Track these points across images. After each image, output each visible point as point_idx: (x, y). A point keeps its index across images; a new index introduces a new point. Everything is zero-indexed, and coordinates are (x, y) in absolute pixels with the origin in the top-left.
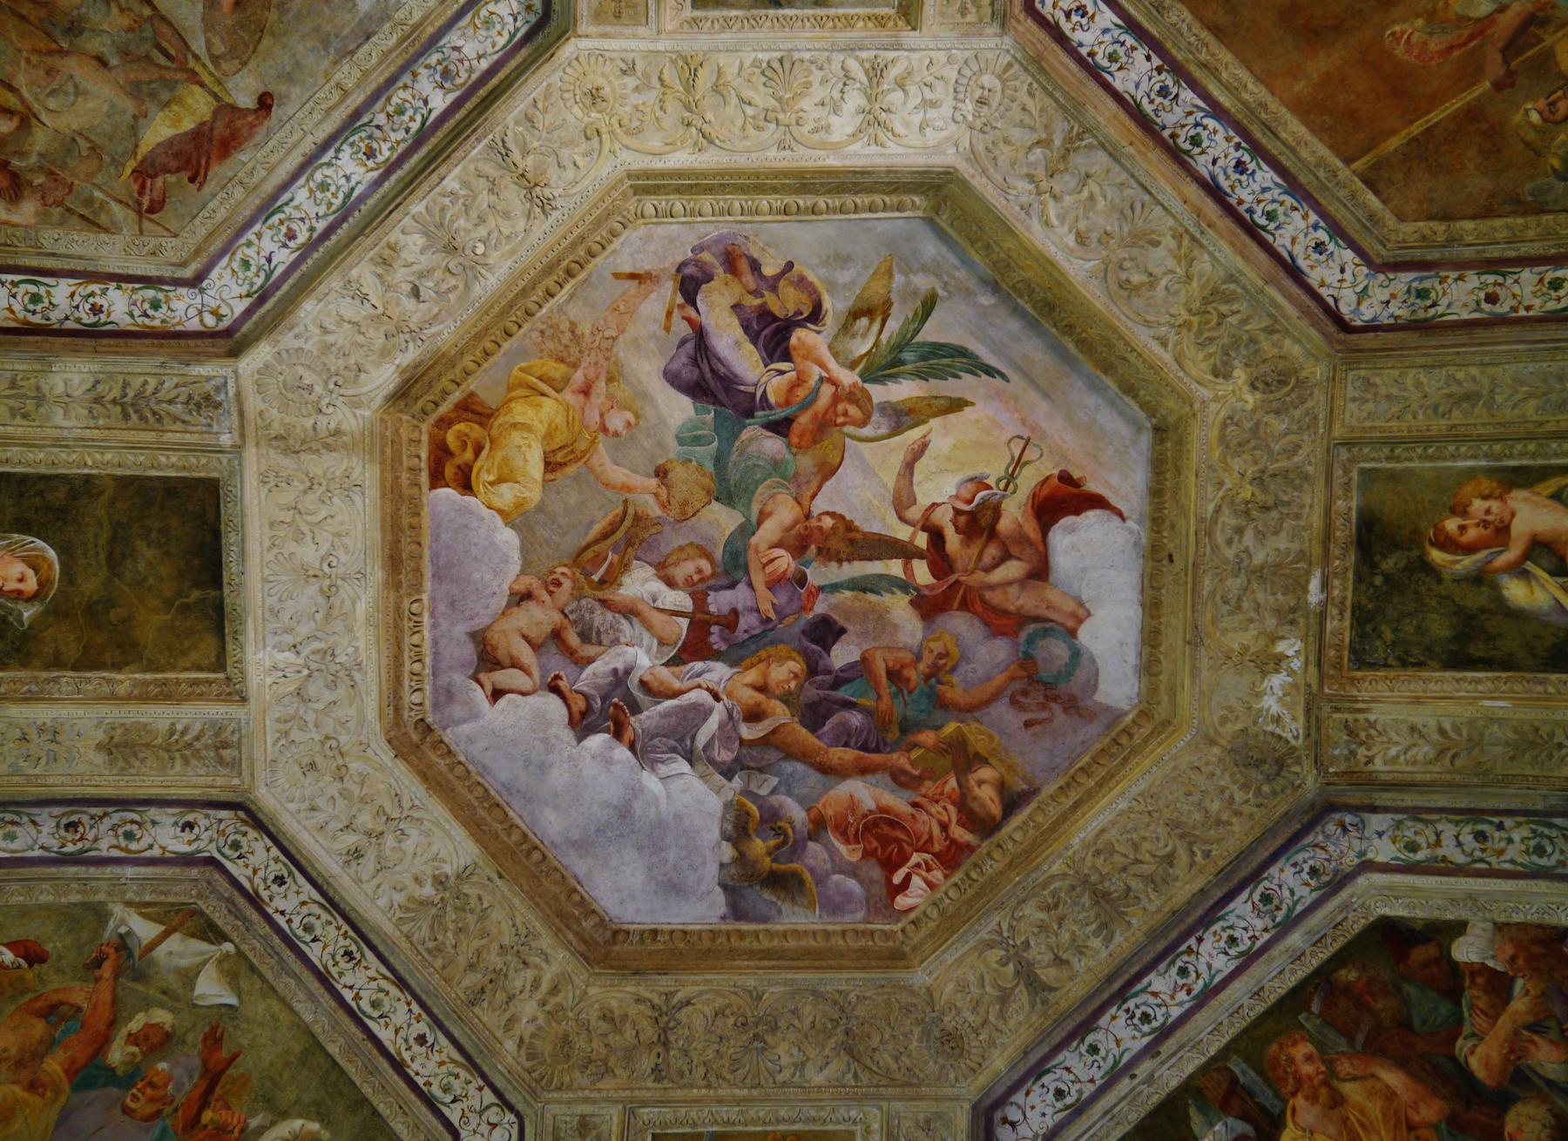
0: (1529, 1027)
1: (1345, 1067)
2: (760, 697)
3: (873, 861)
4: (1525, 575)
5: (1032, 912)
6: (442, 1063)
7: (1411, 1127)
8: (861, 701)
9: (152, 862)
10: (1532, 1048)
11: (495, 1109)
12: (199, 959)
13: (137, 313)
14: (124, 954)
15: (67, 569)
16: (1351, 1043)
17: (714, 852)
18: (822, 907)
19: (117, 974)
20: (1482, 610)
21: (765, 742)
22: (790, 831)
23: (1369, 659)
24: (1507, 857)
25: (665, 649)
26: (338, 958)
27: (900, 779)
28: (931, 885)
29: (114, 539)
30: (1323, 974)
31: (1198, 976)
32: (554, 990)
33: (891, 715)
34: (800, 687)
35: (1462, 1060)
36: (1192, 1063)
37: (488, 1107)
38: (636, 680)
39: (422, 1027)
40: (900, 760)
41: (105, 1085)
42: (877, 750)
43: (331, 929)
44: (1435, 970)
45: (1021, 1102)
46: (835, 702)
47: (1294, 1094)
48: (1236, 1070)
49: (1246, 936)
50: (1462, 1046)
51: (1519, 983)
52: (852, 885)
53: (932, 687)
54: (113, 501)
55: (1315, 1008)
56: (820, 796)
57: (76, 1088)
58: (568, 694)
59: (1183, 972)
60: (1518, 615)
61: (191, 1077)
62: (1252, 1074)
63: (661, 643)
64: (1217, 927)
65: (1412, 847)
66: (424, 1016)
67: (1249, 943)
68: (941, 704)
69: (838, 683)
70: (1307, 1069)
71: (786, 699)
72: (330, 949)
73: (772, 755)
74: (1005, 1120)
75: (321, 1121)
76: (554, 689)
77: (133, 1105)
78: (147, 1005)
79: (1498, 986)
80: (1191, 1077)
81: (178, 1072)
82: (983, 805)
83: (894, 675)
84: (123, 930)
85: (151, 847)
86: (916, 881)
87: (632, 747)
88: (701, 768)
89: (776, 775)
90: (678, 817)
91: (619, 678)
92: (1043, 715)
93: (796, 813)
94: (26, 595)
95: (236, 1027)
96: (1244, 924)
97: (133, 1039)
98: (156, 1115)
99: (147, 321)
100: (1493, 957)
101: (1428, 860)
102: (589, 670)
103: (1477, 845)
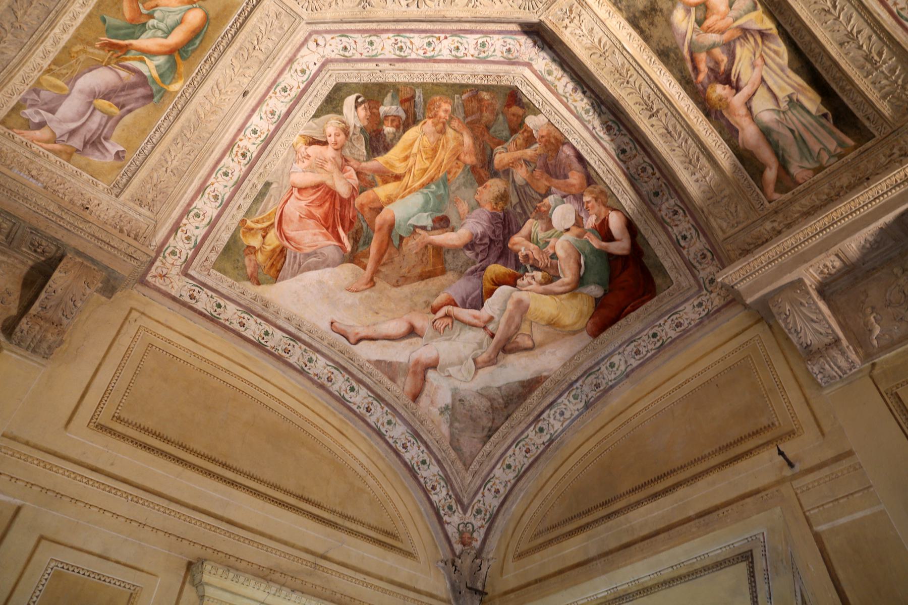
0: (525, 161)
1: (455, 124)
4: (688, 11)
7: (458, 159)
10: (520, 167)
16: (466, 117)
20: (661, 10)
24: (575, 104)
36: (402, 78)
44: (515, 119)
45: (327, 40)
47: (430, 118)
48: (417, 94)
49: (463, 51)
50: (499, 149)
51: (537, 145)
55: (464, 97)
59: (429, 44)
60: (669, 24)
62: (422, 100)
64: (456, 39)
65: (550, 73)
67: (462, 55)
70: (442, 114)
79: (530, 140)
96: (467, 47)
100: (537, 131)
101: (550, 82)
103: (571, 92)
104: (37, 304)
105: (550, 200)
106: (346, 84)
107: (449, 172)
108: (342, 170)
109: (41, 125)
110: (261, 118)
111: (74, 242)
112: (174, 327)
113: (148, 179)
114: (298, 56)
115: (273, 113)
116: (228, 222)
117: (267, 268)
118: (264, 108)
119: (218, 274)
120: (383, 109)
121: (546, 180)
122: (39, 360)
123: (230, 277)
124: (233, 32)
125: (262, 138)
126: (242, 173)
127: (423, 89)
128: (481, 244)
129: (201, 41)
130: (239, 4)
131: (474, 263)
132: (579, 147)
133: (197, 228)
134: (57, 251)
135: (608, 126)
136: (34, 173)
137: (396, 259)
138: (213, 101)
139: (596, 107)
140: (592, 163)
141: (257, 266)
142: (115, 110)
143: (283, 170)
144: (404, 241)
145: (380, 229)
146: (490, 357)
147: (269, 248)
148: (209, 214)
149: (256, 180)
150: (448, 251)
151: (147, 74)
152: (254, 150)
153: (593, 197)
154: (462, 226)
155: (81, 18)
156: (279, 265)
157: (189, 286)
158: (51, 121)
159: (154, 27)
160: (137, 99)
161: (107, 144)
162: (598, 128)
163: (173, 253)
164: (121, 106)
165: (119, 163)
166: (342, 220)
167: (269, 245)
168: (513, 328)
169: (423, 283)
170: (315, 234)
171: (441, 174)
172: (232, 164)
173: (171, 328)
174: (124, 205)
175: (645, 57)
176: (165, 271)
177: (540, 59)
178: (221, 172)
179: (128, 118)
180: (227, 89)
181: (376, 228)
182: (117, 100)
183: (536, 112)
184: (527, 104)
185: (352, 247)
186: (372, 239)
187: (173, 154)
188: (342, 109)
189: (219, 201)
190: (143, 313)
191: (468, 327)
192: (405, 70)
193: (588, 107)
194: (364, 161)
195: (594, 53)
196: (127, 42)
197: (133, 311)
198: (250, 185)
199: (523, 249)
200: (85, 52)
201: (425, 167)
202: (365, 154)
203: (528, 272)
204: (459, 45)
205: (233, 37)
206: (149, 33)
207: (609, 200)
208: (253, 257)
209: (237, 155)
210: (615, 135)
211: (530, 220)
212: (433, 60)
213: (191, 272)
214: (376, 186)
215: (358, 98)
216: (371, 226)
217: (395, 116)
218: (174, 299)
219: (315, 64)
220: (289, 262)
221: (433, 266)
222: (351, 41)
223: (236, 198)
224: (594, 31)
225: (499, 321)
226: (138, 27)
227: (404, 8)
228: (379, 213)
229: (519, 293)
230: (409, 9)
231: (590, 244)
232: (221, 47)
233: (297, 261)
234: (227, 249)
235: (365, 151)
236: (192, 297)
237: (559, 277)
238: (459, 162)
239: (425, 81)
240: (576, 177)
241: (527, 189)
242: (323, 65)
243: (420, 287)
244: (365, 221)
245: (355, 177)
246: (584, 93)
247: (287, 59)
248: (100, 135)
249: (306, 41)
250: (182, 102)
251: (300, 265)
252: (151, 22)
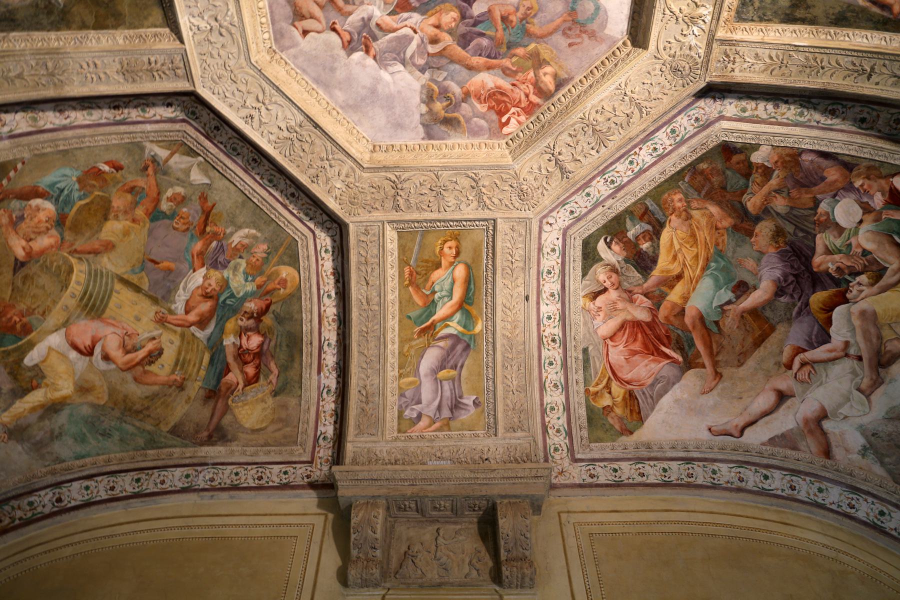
1: (695, 204)
2: (436, 31)
3: (493, 112)
5: (565, 138)
6: (303, 205)
7: (717, 229)
8: (488, 33)
9: (157, 122)
10: (774, 199)
11: (329, 222)
12: (190, 164)
14: (156, 164)
16: (699, 193)
17: (417, 108)
18: (469, 132)
19: (155, 173)
21: (440, 54)
22: (453, 98)
23: (744, 16)
25: (388, 6)
26: (250, 161)
27: (506, 72)
28: (519, 122)
30: (692, 167)
31: (637, 165)
32: (347, 176)
33: (503, 40)
34: (457, 26)
35: (744, 203)
36: (629, 201)
37: (326, 221)
38: (374, 23)
39: (292, 190)
40: (506, 62)
41: (163, 218)
42: (495, 58)
43: (245, 150)
44: (742, 165)
45: (555, 216)
46: (475, 33)
47: (671, 214)
48: (648, 204)
49: (661, 148)
52: (483, 122)
53: (523, 25)
55: (686, 179)
56: (467, 81)
57: (152, 221)
58: (340, 32)
59: (631, 163)
61: (198, 214)
63: (385, 3)
64: (649, 143)
66: (293, 185)
68: (527, 34)
69: (475, 25)
70: (679, 204)
71: (450, 32)
72: (246, 158)
73: (444, 61)
74: (548, 223)
75: (256, 229)
76: (334, 30)
77: (177, 226)
78: (172, 186)
80: (629, 207)
81: (192, 212)
82: (546, 85)
83: (504, 19)
84: (152, 153)
85: (155, 115)
86: (513, 121)
87: (375, 58)
88: (409, 68)
89: (446, 71)
90: (399, 92)
91: (366, 22)
92: (578, 40)
93: (456, 90)
95: (212, 193)
96: (661, 142)
97: (169, 199)
98: (188, 229)
102: (350, 19)
104: (502, 551)
105: (823, 207)
106: (590, 236)
107: (717, 244)
108: (632, 301)
109: (420, 416)
110: (547, 305)
111: (495, 491)
112: (596, 509)
113: (506, 408)
114: (543, 242)
115: (552, 295)
116: (576, 399)
117: (629, 416)
118: (544, 296)
119: (597, 444)
120: (630, 234)
121: (806, 193)
122: (529, 591)
123: (607, 441)
124: (490, 263)
125: (558, 319)
126: (561, 355)
127: (650, 197)
128: (789, 285)
129: (474, 284)
130: (482, 241)
131: (794, 305)
132: (817, 148)
133: (559, 418)
134: (488, 503)
135: (830, 110)
136: (438, 454)
137: (725, 343)
138: (510, 320)
139: (807, 105)
140: (839, 151)
141: (621, 419)
142: (453, 373)
143: (589, 332)
144: (721, 323)
145: (694, 327)
146: (872, 379)
147: (619, 399)
148: (559, 402)
149: (575, 354)
150: (764, 308)
151: (455, 333)
152: (558, 331)
153: (864, 178)
154: (760, 280)
155: (397, 326)
156: (636, 407)
157: (584, 468)
158: (423, 409)
159: (440, 298)
160: (461, 355)
161: (464, 401)
162: (823, 120)
163: (556, 450)
164: (454, 367)
165: (480, 409)
166: (659, 339)
167: (618, 397)
168: (874, 340)
169: (762, 348)
170: (646, 365)
171: (712, 251)
172: (550, 353)
173: (595, 512)
174: (505, 438)
175: (824, 36)
176: (560, 467)
177: (728, 107)
178: (546, 365)
179: (464, 372)
180: (513, 304)
181: (690, 328)
182: (450, 365)
183: (756, 147)
184: (742, 147)
185: (682, 356)
186: (693, 339)
187: (509, 377)
188: (600, 256)
189: (560, 387)
190: (568, 512)
191: (830, 363)
192: (627, 194)
193: (799, 110)
194: (644, 283)
195: (773, 70)
196: (431, 321)
197: (561, 514)
198: (574, 360)
199: (830, 265)
200: (411, 347)
201: (695, 253)
202: (641, 277)
203: (851, 282)
204: (655, 146)
205: (493, 266)
206: (440, 304)
207: (882, 170)
208: (612, 414)
209: (548, 344)
210: (843, 113)
211: (818, 236)
212: (642, 171)
213: (578, 456)
214: (667, 295)
215: (605, 240)
216: (685, 329)
217: (643, 233)
218: (581, 486)
219: (558, 239)
220: (642, 400)
221: (760, 329)
222: (572, 204)
223: (570, 377)
224: (760, 54)
225: (856, 342)
226: (431, 306)
227: (597, 155)
228: (684, 315)
229: (856, 305)
230: (600, 153)
231: (894, 220)
232: (490, 278)
233: (648, 395)
234: (590, 420)
235: (639, 275)
236: (592, 476)
237: (886, 269)
238: (719, 231)
239: (647, 191)
240: (833, 172)
241: (795, 212)
242: (564, 235)
243: (761, 354)
244: (677, 329)
245: (645, 299)
246: (786, 102)
247: (536, 250)
248: (456, 397)
249: (541, 228)
250: (490, 335)
251: (652, 397)
252: (436, 296)
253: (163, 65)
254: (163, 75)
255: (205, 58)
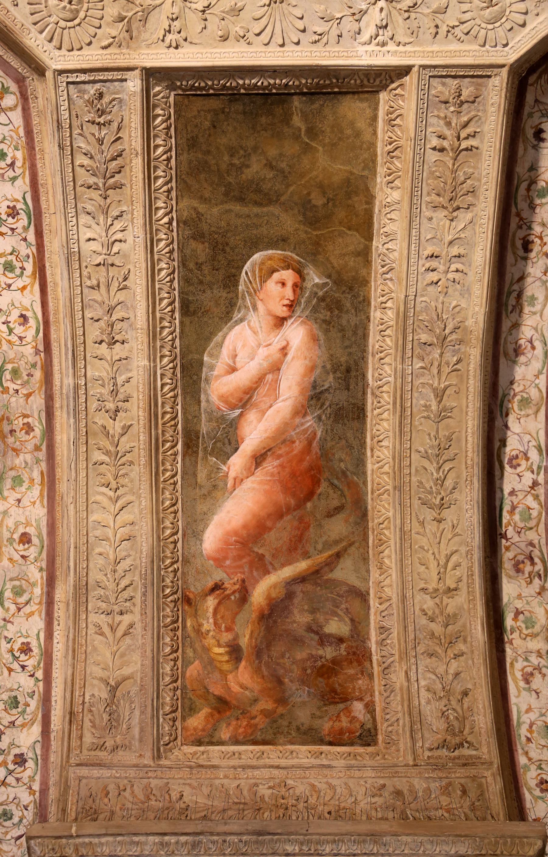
13: (11, 174)
15: (272, 244)
29: (241, 200)
54: (203, 199)
94: (298, 280)
99: (19, 164)
253: (448, 124)
254: (469, 130)
255: (443, 29)
